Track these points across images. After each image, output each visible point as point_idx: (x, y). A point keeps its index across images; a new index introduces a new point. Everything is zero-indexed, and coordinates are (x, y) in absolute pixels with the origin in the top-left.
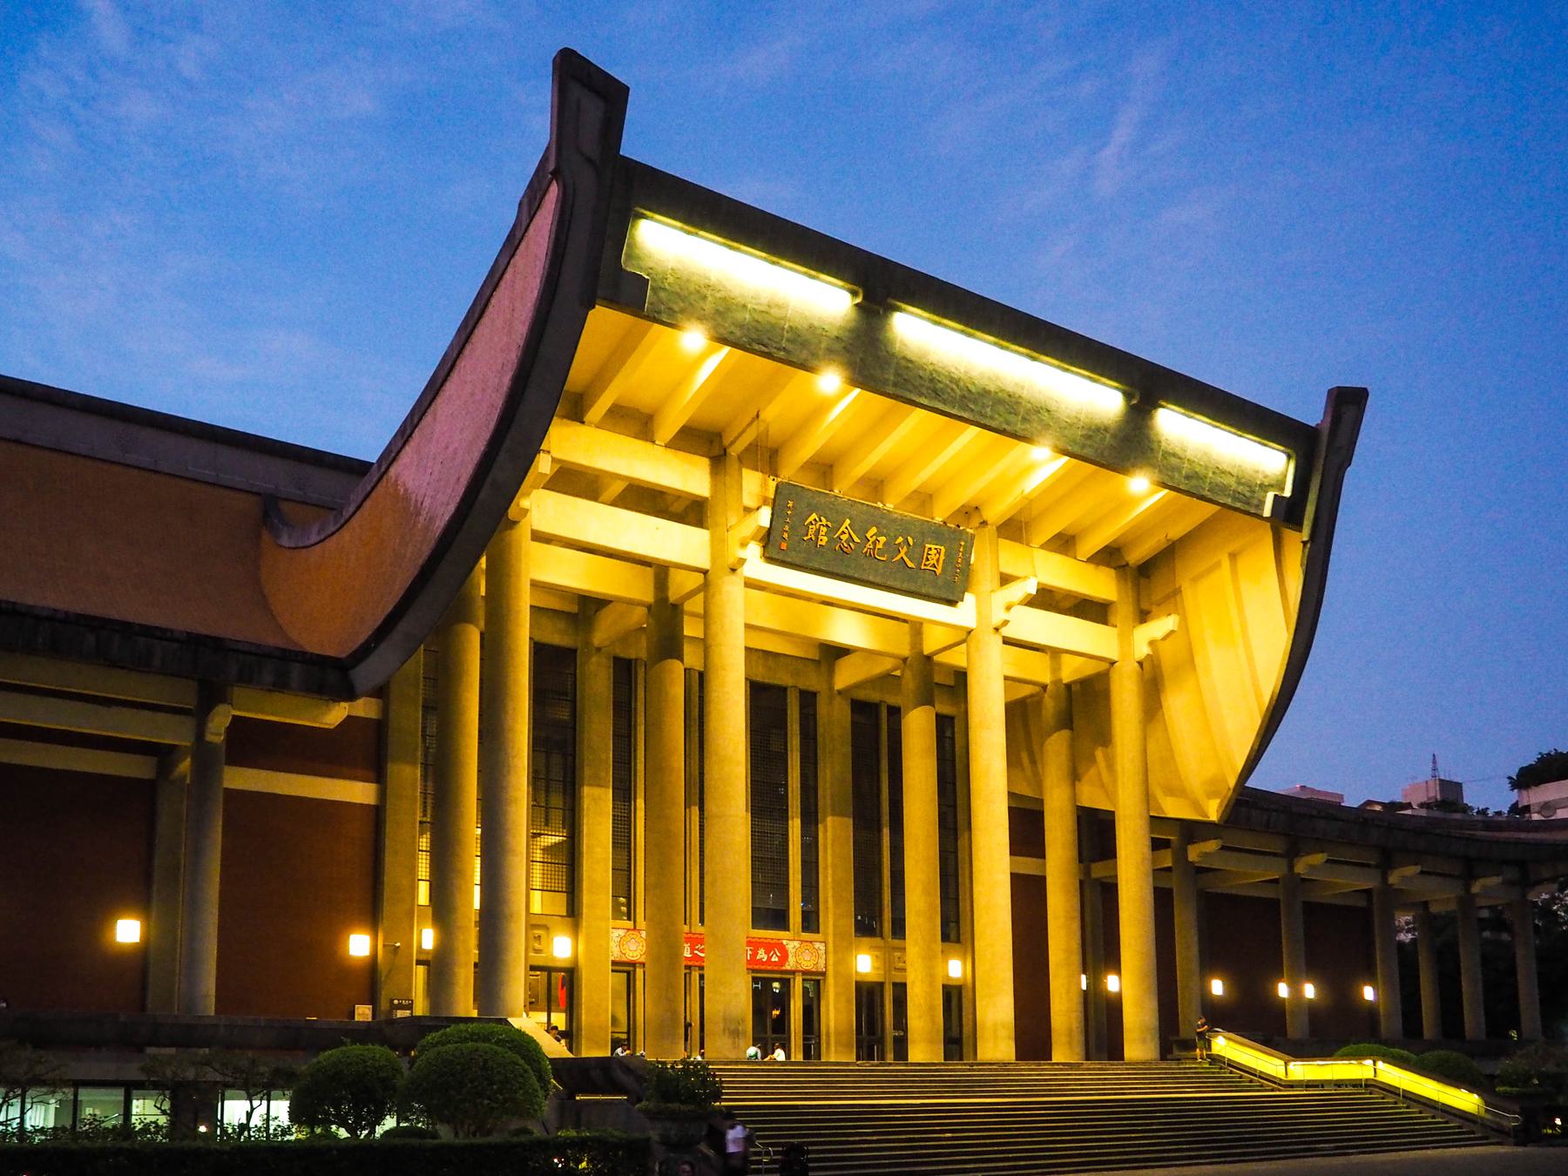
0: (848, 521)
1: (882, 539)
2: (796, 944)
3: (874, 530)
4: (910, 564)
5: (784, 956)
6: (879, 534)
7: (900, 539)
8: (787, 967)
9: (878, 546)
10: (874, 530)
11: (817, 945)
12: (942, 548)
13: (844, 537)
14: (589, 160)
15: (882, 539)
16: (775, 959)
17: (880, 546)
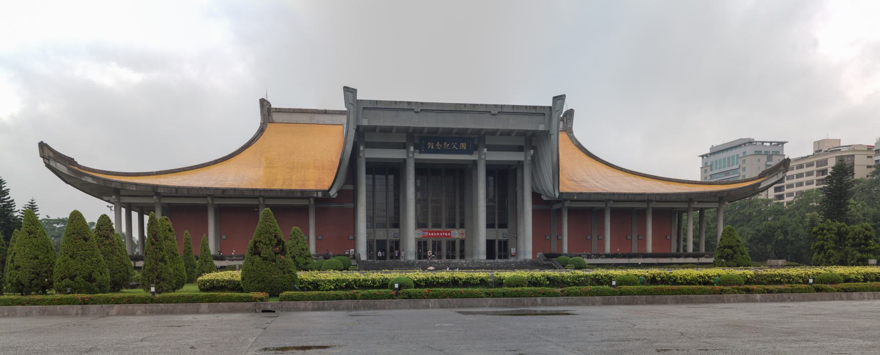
1: (448, 144)
7: (453, 144)
15: (448, 144)
17: (448, 146)
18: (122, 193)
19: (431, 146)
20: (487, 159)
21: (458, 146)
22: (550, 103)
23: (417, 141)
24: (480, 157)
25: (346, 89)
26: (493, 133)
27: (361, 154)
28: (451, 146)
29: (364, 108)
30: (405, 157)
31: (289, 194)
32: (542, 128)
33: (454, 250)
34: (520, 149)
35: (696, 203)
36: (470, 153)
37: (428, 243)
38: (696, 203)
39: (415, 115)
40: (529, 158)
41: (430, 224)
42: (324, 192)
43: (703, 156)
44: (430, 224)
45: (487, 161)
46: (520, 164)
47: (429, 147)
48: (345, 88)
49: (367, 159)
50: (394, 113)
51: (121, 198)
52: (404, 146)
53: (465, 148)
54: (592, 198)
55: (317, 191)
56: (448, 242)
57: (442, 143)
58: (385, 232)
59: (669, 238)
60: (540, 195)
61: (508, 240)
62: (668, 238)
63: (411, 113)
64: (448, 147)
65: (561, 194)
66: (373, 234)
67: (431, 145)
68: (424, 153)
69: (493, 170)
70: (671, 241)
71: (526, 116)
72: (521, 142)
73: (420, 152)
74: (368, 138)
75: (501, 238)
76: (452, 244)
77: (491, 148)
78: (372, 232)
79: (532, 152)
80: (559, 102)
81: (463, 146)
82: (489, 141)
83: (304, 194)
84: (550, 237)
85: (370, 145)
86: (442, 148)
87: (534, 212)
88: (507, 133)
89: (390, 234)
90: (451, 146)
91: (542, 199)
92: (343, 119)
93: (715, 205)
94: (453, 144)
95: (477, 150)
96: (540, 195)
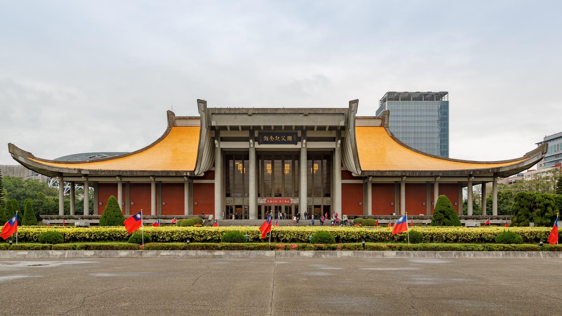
0: (271, 136)
1: (279, 138)
2: (293, 199)
3: (277, 136)
4: (285, 140)
5: (290, 201)
6: (278, 137)
7: (282, 137)
8: (291, 203)
9: (278, 139)
10: (277, 136)
11: (297, 199)
12: (291, 137)
13: (271, 139)
14: (203, 111)
15: (279, 138)
16: (288, 202)
17: (278, 139)
18: (64, 175)
19: (266, 139)
20: (308, 147)
21: (286, 138)
22: (347, 106)
24: (302, 146)
25: (201, 103)
26: (312, 128)
27: (217, 146)
28: (281, 139)
29: (213, 114)
30: (248, 147)
31: (166, 174)
32: (342, 123)
33: (290, 213)
34: (333, 140)
35: (473, 178)
36: (296, 144)
37: (272, 207)
38: (473, 178)
39: (249, 117)
40: (339, 146)
42: (191, 172)
45: (308, 149)
46: (333, 151)
47: (265, 139)
48: (198, 100)
49: (222, 149)
50: (233, 116)
51: (64, 178)
52: (246, 140)
53: (291, 140)
54: (100, 174)
55: (186, 172)
57: (275, 137)
58: (242, 200)
59: (457, 205)
60: (351, 173)
61: (330, 205)
62: (455, 204)
63: (246, 116)
64: (279, 139)
65: (363, 172)
66: (232, 201)
67: (266, 138)
68: (262, 143)
69: (313, 155)
70: (458, 207)
71: (330, 116)
72: (333, 134)
73: (259, 144)
74: (223, 134)
76: (288, 209)
77: (309, 140)
78: (232, 200)
79: (339, 141)
80: (354, 105)
81: (290, 138)
82: (310, 134)
83: (178, 174)
84: (363, 204)
85: (223, 140)
86: (274, 140)
88: (321, 128)
89: (245, 201)
90: (281, 139)
91: (352, 176)
92: (198, 123)
93: (491, 179)
94: (282, 137)
95: (300, 141)
96: (351, 173)
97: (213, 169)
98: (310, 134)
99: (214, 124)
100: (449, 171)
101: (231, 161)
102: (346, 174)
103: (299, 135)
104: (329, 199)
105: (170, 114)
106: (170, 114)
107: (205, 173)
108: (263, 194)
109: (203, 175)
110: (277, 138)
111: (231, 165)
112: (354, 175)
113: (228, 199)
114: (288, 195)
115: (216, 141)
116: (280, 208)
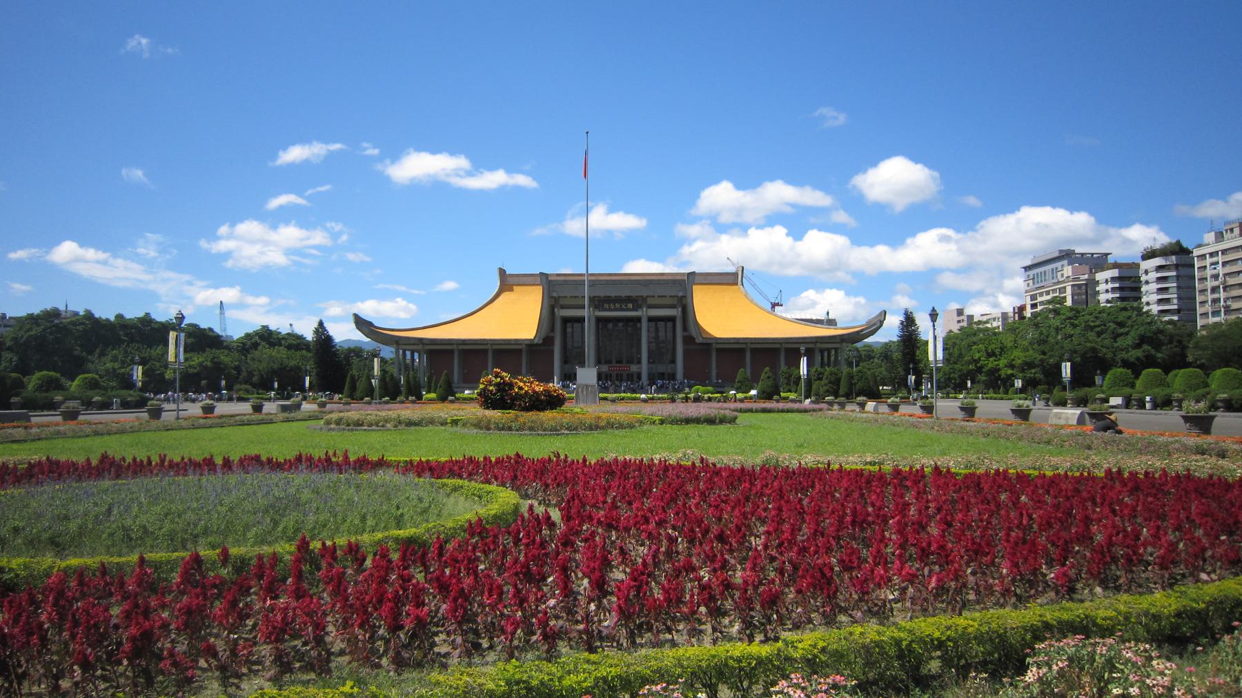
21: (626, 306)
23: (597, 303)
28: (621, 306)
32: (680, 294)
40: (680, 313)
41: (614, 362)
43: (1027, 268)
44: (614, 362)
56: (628, 375)
67: (606, 306)
72: (675, 301)
74: (562, 302)
75: (669, 371)
79: (680, 309)
81: (630, 306)
85: (563, 307)
87: (686, 352)
90: (621, 306)
97: (551, 334)
98: (650, 301)
99: (555, 295)
100: (791, 338)
101: (569, 325)
102: (689, 340)
103: (640, 302)
104: (673, 365)
105: (502, 272)
106: (502, 272)
107: (544, 340)
108: (603, 361)
109: (541, 342)
110: (618, 305)
111: (569, 330)
112: (697, 341)
113: (566, 366)
114: (630, 362)
115: (556, 310)
116: (621, 375)
